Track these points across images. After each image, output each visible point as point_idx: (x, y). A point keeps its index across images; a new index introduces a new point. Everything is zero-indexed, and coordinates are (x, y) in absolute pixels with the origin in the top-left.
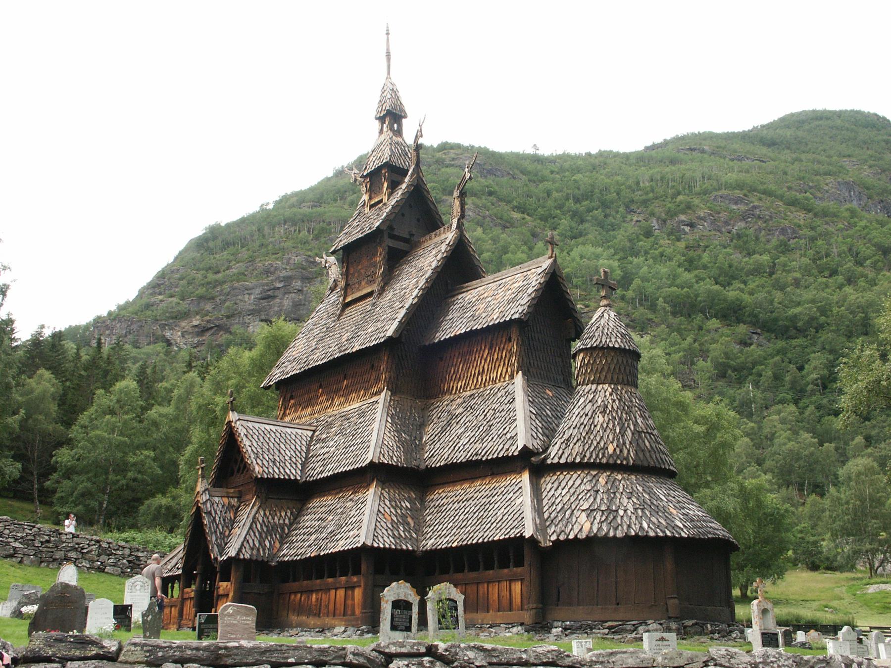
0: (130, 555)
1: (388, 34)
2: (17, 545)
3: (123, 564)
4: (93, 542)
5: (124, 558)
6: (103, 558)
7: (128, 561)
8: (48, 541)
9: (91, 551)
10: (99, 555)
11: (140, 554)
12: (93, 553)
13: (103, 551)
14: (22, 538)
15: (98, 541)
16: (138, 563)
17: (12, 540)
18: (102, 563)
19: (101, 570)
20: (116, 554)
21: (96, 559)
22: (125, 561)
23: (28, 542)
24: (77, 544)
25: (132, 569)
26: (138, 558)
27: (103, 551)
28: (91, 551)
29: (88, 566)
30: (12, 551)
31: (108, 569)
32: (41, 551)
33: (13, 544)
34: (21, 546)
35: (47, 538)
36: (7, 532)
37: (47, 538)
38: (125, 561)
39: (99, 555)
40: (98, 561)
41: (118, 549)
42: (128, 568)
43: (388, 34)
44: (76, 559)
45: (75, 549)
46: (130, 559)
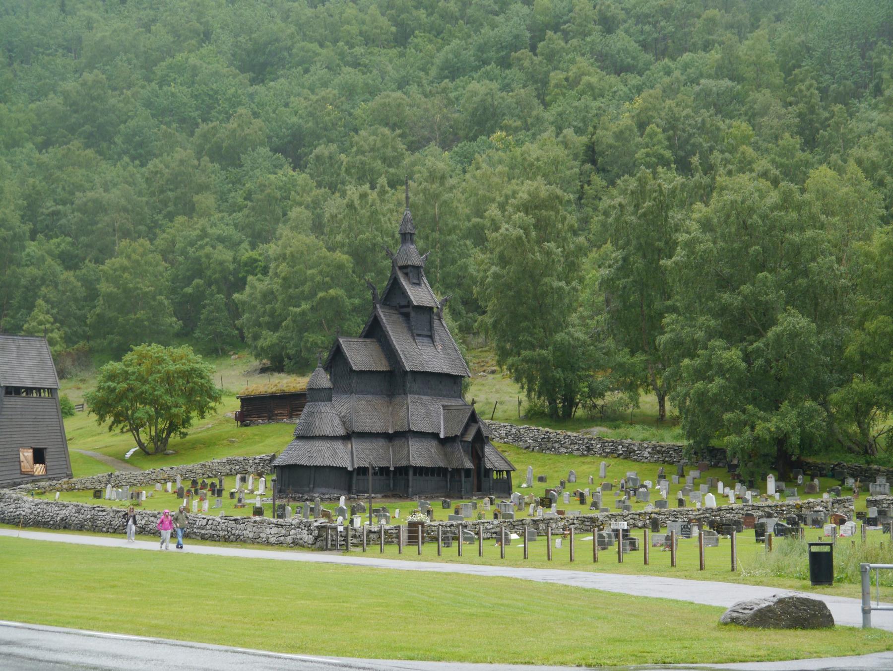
19: (571, 453)
23: (535, 440)
26: (592, 445)
45: (556, 442)
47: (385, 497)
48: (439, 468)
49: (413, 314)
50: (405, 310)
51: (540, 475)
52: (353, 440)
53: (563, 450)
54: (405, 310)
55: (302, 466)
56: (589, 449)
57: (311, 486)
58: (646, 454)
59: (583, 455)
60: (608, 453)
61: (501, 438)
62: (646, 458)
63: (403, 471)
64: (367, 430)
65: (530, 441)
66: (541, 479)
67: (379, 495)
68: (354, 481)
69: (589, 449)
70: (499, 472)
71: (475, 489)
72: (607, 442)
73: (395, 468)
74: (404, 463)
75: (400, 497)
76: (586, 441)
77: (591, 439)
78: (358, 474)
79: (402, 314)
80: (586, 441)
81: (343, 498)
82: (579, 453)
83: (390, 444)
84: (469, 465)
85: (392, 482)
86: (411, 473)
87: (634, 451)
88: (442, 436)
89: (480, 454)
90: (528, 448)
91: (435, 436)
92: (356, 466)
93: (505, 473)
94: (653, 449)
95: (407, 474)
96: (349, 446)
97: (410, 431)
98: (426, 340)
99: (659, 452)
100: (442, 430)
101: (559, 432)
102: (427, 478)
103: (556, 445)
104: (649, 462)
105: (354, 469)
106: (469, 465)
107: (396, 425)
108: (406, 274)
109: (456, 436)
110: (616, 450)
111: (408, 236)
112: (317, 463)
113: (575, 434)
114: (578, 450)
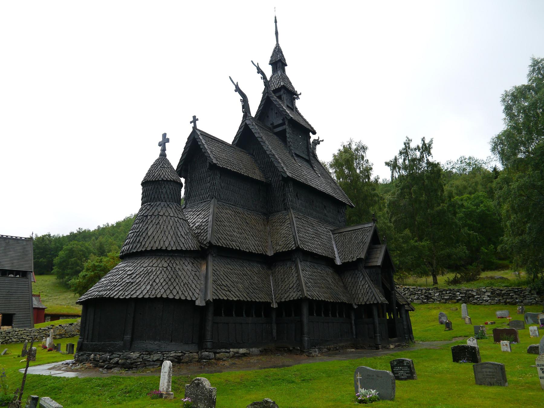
0: (426, 293)
1: (276, 22)
3: (422, 298)
4: (406, 289)
5: (422, 295)
6: (412, 296)
7: (425, 296)
9: (406, 294)
10: (410, 295)
11: (430, 292)
12: (407, 294)
15: (408, 289)
16: (430, 296)
18: (411, 299)
20: (417, 294)
21: (409, 297)
25: (428, 300)
26: (430, 294)
28: (406, 294)
39: (410, 295)
40: (409, 298)
41: (419, 291)
43: (276, 22)
46: (426, 295)
47: (265, 352)
52: (210, 258)
55: (110, 300)
56: (428, 298)
57: (128, 337)
58: (486, 298)
59: (423, 303)
62: (487, 301)
64: (234, 245)
67: (255, 350)
68: (209, 328)
69: (428, 298)
73: (280, 304)
74: (294, 295)
75: (290, 351)
76: (424, 291)
77: (429, 289)
78: (217, 313)
79: (278, 134)
80: (424, 291)
82: (420, 301)
83: (270, 272)
84: (382, 299)
85: (275, 327)
87: (473, 296)
88: (338, 262)
91: (329, 261)
92: (210, 297)
94: (492, 293)
96: (204, 268)
97: (298, 250)
99: (499, 295)
100: (337, 255)
104: (490, 304)
105: (208, 302)
106: (382, 299)
107: (277, 244)
108: (280, 97)
109: (359, 260)
110: (455, 296)
111: (280, 64)
112: (138, 294)
114: (418, 299)
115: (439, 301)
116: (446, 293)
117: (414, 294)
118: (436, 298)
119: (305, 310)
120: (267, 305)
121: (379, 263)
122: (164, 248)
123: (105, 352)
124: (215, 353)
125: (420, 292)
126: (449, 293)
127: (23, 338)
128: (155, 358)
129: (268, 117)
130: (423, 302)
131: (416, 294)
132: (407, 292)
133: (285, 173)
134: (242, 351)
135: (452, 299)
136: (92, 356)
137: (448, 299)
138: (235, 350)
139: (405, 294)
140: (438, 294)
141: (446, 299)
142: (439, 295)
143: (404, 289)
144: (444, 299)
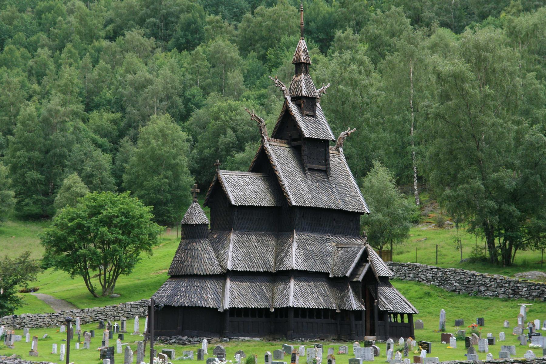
2: (456, 284)
3: (508, 292)
5: (509, 288)
7: (512, 290)
8: (470, 281)
11: (519, 285)
13: (499, 286)
14: (458, 280)
15: (495, 279)
16: (517, 291)
17: (454, 282)
19: (497, 296)
21: (494, 290)
22: (510, 290)
23: (461, 283)
24: (484, 281)
27: (499, 286)
29: (491, 294)
30: (454, 288)
31: (501, 296)
32: (467, 287)
33: (455, 284)
34: (458, 285)
35: (469, 279)
36: (452, 277)
37: (469, 279)
38: (510, 290)
39: (496, 288)
41: (506, 283)
42: (512, 294)
44: (484, 291)
45: (482, 285)
48: (326, 310)
49: (304, 148)
50: (296, 143)
51: (457, 319)
53: (489, 293)
54: (296, 143)
60: (534, 297)
61: (428, 281)
63: (285, 312)
65: (456, 284)
66: (458, 323)
70: (395, 314)
71: (368, 332)
72: (534, 285)
76: (512, 284)
77: (518, 282)
81: (205, 341)
82: (505, 296)
86: (292, 315)
89: (374, 295)
90: (454, 291)
92: (227, 306)
93: (399, 316)
95: (287, 316)
98: (320, 176)
101: (486, 274)
102: (312, 320)
103: (482, 288)
105: (225, 311)
108: (299, 106)
113: (501, 277)
114: (504, 293)
115: (527, 298)
116: (535, 289)
117: (501, 287)
118: (523, 293)
119: (292, 315)
120: (267, 310)
121: (360, 278)
122: (199, 274)
123: (167, 336)
124: (230, 339)
125: (507, 285)
126: (539, 289)
127: (37, 324)
128: (196, 340)
129: (287, 127)
130: (509, 298)
131: (502, 286)
132: (493, 283)
133: (291, 203)
134: (247, 339)
135: (540, 297)
136: (158, 338)
137: (536, 296)
138: (243, 338)
139: (491, 286)
140: (526, 289)
141: (534, 296)
142: (527, 290)
143: (491, 279)
144: (531, 296)
